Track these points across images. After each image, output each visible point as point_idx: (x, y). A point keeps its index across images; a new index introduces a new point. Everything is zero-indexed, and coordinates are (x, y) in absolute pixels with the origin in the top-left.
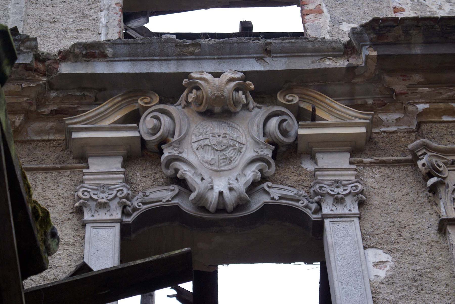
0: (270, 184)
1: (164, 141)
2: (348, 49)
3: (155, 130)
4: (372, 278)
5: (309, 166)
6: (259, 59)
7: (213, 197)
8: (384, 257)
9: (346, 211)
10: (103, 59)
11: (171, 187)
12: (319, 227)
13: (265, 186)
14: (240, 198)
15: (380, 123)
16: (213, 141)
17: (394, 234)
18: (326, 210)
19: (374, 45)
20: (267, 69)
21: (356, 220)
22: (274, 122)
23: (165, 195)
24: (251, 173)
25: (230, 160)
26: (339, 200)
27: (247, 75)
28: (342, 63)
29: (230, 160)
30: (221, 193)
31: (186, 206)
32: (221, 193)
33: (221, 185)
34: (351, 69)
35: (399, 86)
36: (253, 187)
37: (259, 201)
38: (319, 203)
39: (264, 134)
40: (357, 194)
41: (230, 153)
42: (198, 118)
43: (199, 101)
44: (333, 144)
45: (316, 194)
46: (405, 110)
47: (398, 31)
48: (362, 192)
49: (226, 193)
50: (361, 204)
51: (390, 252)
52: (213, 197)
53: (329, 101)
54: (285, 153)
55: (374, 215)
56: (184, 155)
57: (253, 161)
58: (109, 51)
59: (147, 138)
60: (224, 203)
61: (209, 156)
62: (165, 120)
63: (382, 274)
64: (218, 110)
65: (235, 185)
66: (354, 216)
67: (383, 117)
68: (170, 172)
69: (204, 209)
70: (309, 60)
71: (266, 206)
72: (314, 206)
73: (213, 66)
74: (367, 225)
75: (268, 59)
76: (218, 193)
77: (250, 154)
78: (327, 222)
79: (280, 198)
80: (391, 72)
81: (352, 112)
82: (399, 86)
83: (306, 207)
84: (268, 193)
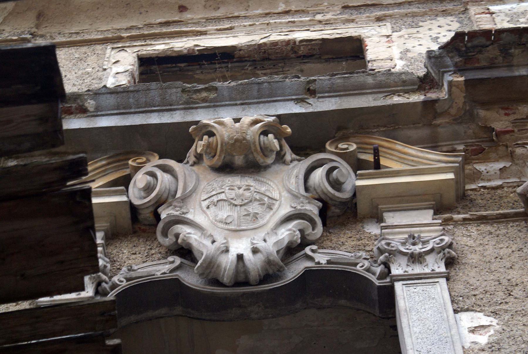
0: (314, 247)
1: (160, 202)
2: (425, 83)
3: (148, 189)
4: (467, 345)
5: (373, 229)
6: (300, 101)
7: (228, 261)
8: (483, 319)
9: (427, 270)
10: (82, 115)
11: (171, 259)
12: (388, 296)
13: (307, 250)
14: (269, 262)
15: (477, 176)
16: (232, 194)
17: (501, 294)
18: (396, 270)
19: (459, 70)
20: (310, 110)
21: (443, 281)
22: (318, 175)
23: (161, 268)
24: (286, 234)
25: (256, 216)
26: (416, 258)
27: (282, 119)
28: (417, 98)
29: (256, 216)
30: (240, 257)
31: (191, 279)
32: (240, 257)
33: (240, 246)
34: (428, 104)
35: (500, 122)
36: (291, 251)
37: (296, 269)
38: (386, 265)
39: (307, 189)
40: (443, 248)
41: (254, 208)
42: (212, 176)
43: (211, 150)
44: (408, 198)
45: (381, 251)
46: (512, 156)
47: (493, 52)
48: (450, 246)
49: (248, 255)
50: (450, 262)
51: (495, 314)
52: (228, 261)
53: (399, 146)
54: (339, 213)
55: (468, 276)
56: (190, 216)
57: (288, 219)
58: (90, 104)
59: (137, 202)
60: (246, 272)
61: (224, 212)
62: (164, 178)
63: (483, 339)
64: (240, 161)
65: (261, 245)
66: (439, 275)
67: (481, 167)
68: (168, 241)
69: (216, 282)
70: (370, 98)
71: (308, 272)
72: (378, 270)
73: (235, 112)
74: (459, 287)
75: (311, 101)
76: (236, 256)
77: (285, 210)
78: (398, 286)
79: (329, 262)
80: (486, 105)
81: (433, 155)
82: (500, 122)
83: (368, 270)
84: (311, 259)
